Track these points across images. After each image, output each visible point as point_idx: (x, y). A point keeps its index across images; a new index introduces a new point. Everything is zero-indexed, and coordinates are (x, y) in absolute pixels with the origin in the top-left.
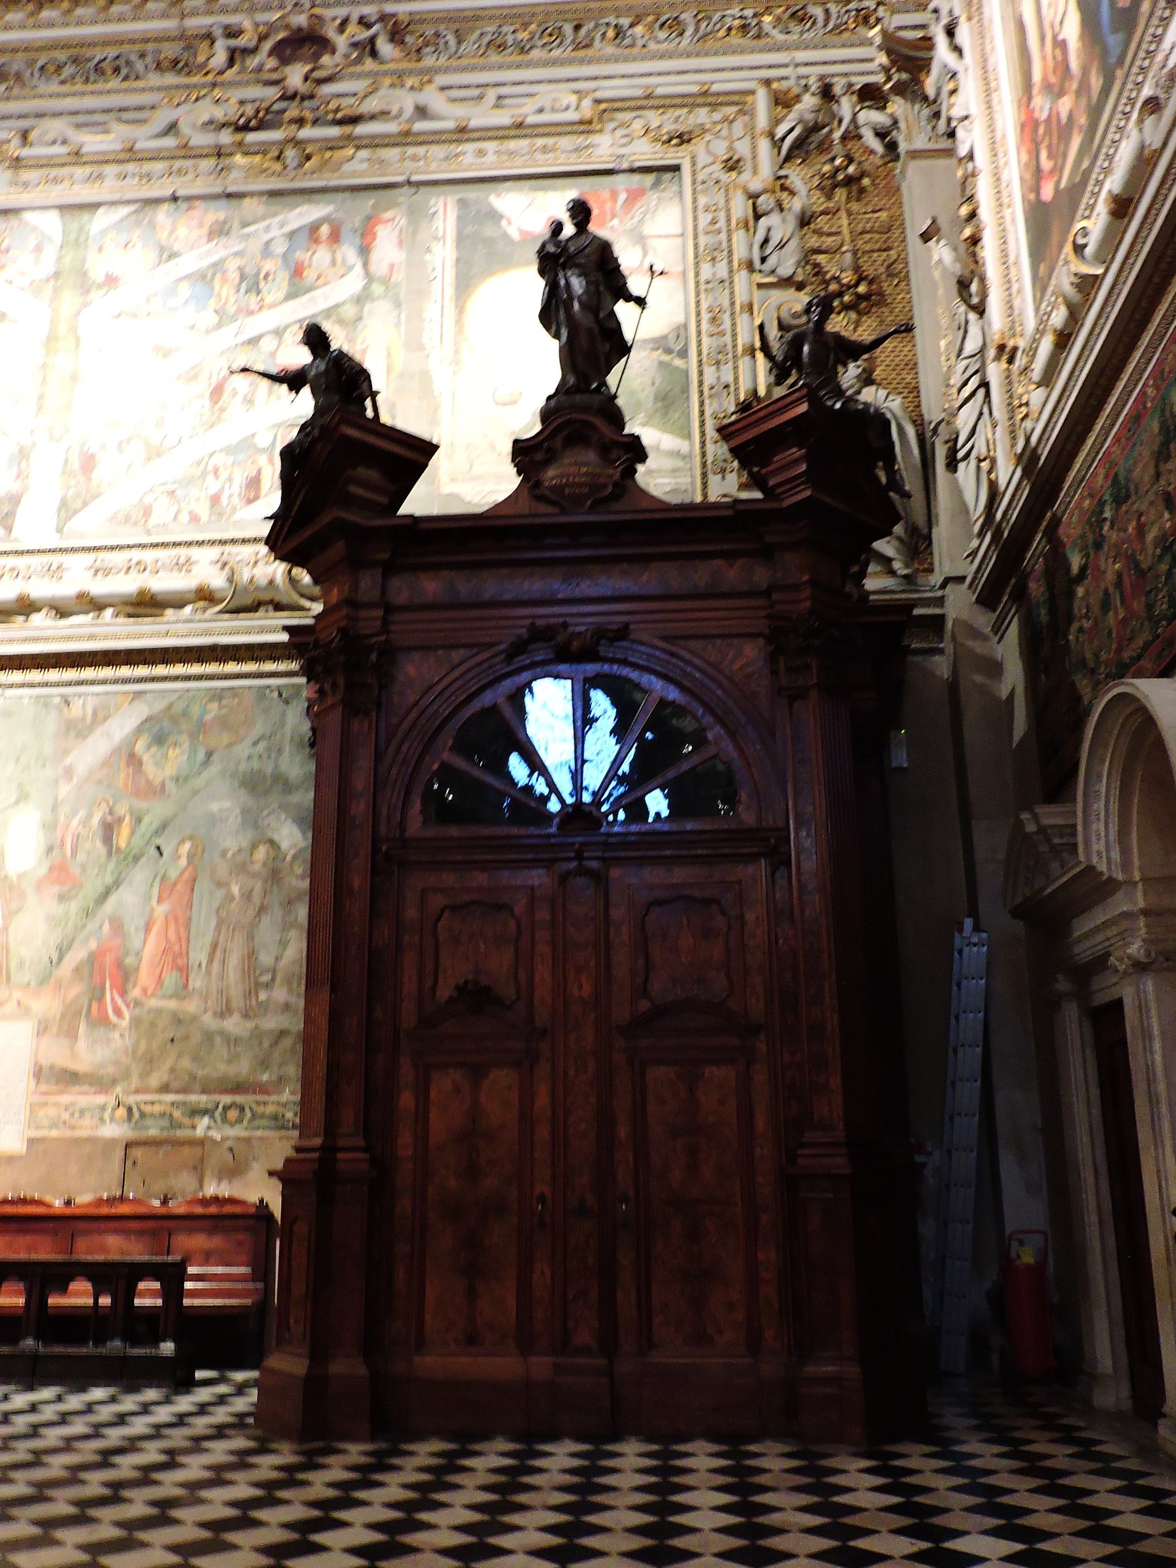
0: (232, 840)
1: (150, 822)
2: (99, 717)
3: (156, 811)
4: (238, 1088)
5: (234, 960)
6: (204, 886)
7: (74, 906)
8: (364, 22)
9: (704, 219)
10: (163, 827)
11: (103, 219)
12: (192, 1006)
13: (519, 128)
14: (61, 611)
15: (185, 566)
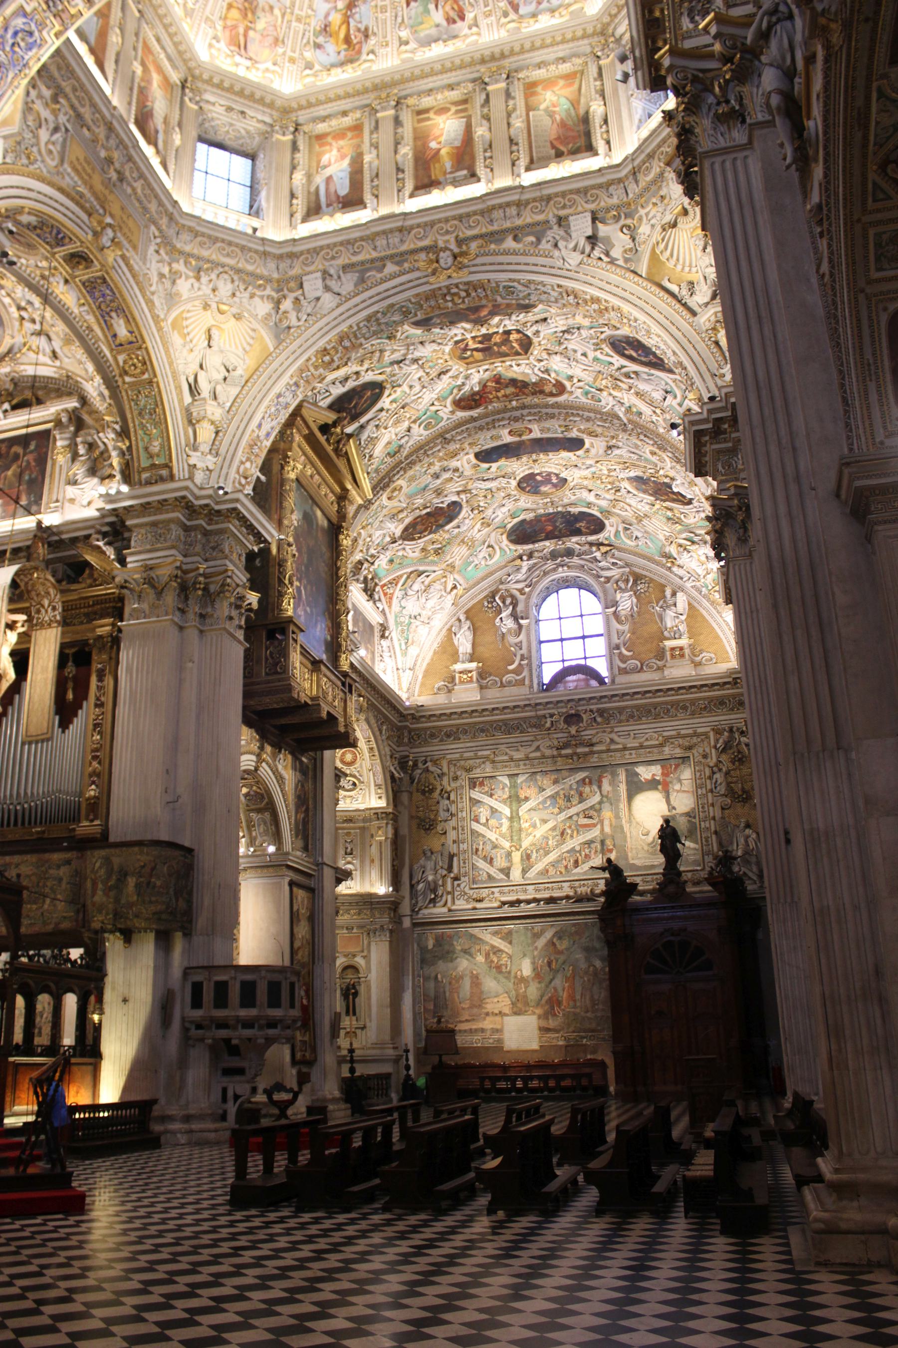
0: (583, 965)
1: (560, 961)
2: (542, 932)
3: (562, 958)
4: (593, 1031)
5: (588, 997)
6: (577, 978)
7: (543, 985)
8: (591, 711)
9: (698, 774)
10: (564, 963)
11: (520, 779)
12: (578, 1010)
13: (641, 747)
14: (528, 902)
15: (561, 888)
